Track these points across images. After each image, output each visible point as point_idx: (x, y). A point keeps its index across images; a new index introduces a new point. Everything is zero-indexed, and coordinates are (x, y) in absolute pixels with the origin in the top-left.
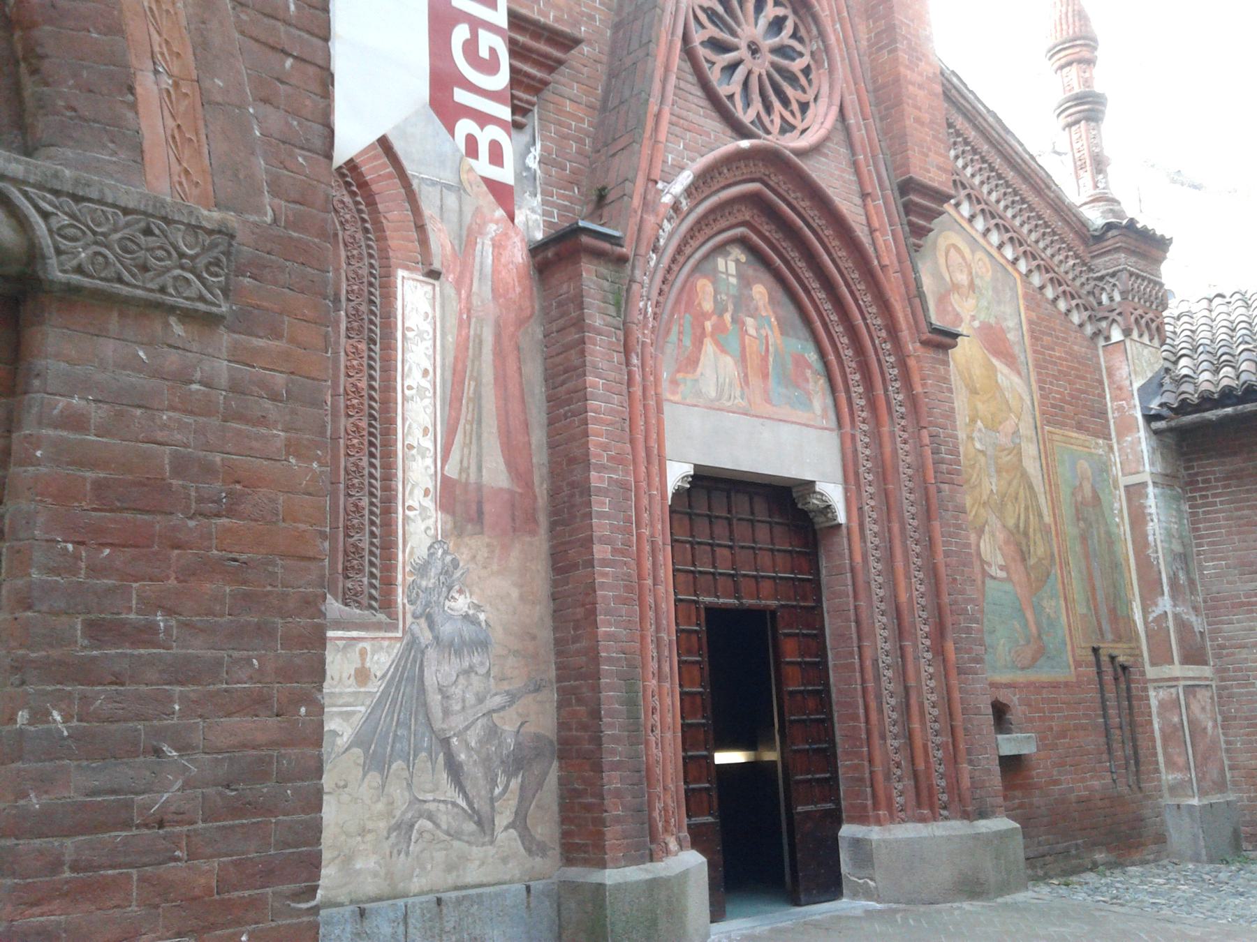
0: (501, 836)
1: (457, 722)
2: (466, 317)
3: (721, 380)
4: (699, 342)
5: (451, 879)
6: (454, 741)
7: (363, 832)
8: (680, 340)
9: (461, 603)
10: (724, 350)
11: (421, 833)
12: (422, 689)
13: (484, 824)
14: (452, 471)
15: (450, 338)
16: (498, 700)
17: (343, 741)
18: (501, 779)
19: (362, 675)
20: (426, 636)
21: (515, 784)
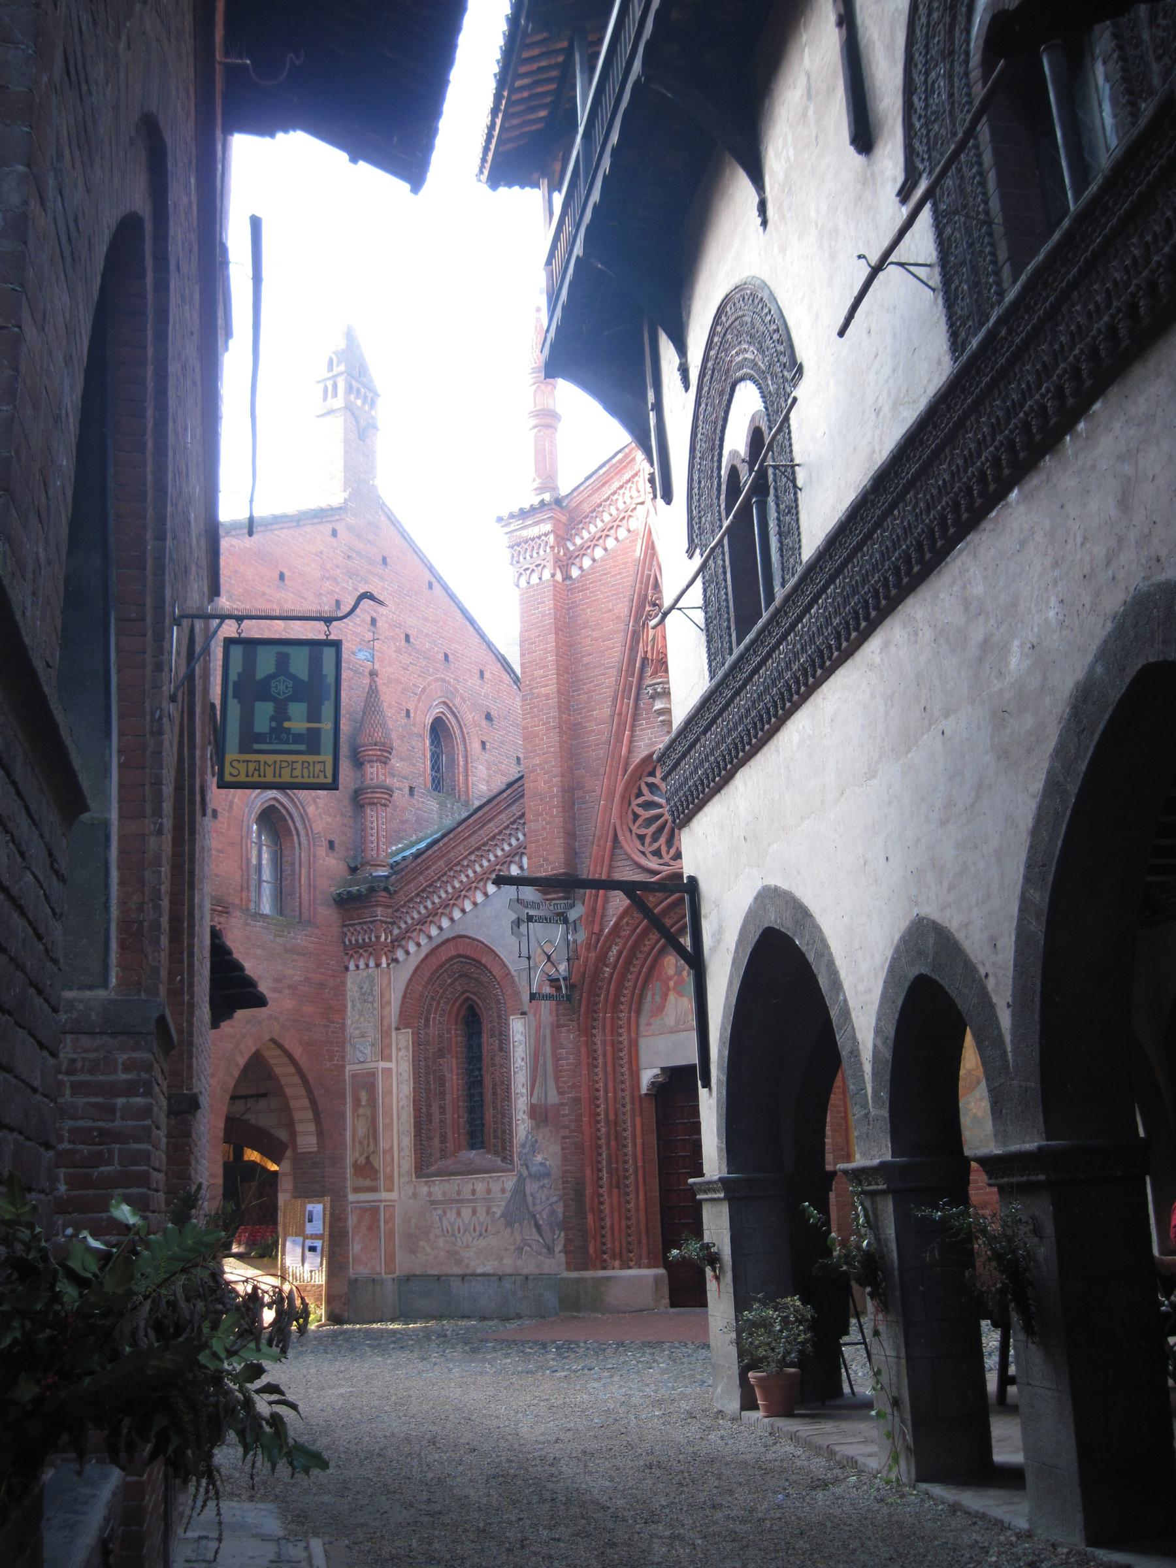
0: (557, 1255)
1: (539, 1208)
2: (538, 1028)
3: (679, 1013)
4: (665, 996)
5: (538, 1272)
6: (538, 1216)
7: (506, 1250)
8: (653, 998)
9: (539, 1158)
10: (680, 994)
11: (526, 1252)
12: (525, 1195)
13: (550, 1250)
14: (534, 1101)
15: (532, 1040)
16: (555, 1199)
17: (498, 1215)
18: (557, 1232)
19: (503, 1191)
20: (525, 1173)
21: (563, 1234)
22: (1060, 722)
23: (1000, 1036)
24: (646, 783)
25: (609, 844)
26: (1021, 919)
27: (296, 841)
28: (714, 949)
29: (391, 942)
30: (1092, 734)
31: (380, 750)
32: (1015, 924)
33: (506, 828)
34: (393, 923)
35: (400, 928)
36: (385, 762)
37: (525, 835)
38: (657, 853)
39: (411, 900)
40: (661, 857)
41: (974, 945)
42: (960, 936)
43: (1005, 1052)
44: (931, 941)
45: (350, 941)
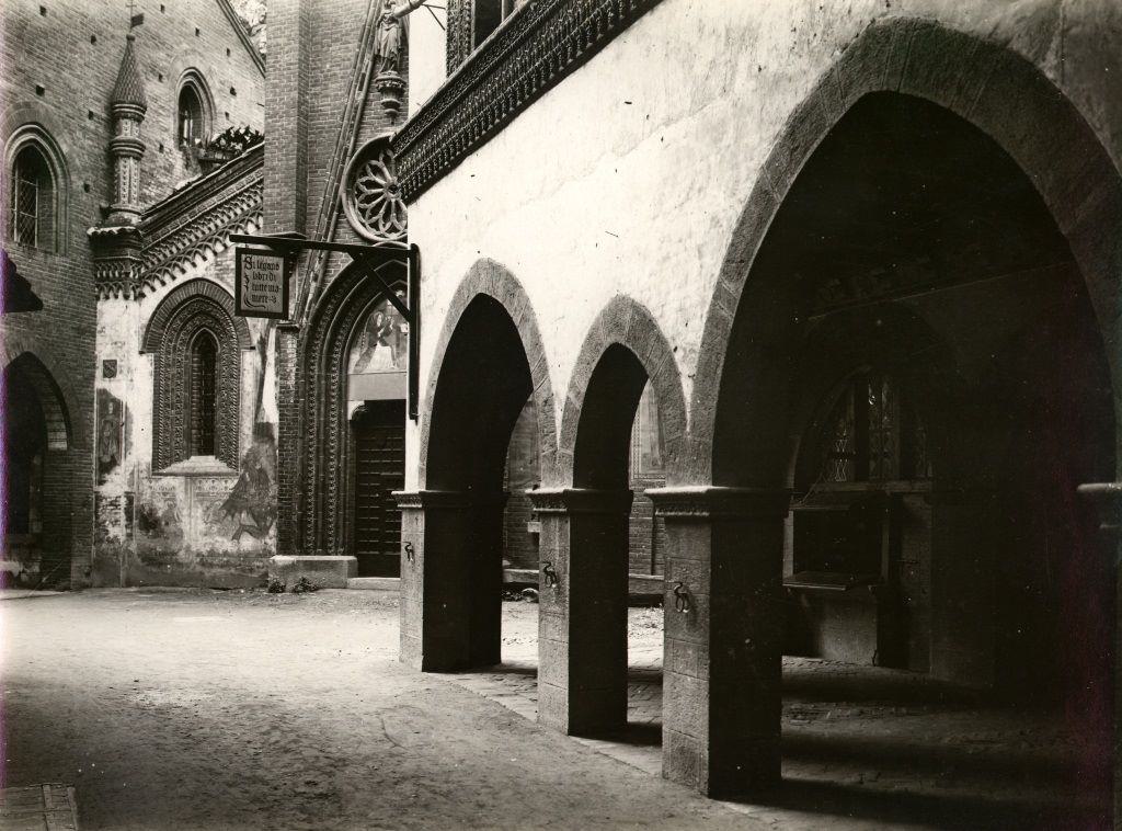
10: (385, 344)
22: (775, 138)
23: (682, 398)
24: (371, 166)
25: (335, 213)
26: (713, 305)
27: (54, 182)
28: (430, 307)
29: (140, 278)
30: (805, 152)
31: (135, 109)
32: (707, 308)
33: (246, 191)
34: (139, 263)
35: (147, 267)
36: (139, 120)
37: (262, 198)
38: (375, 226)
39: (158, 245)
40: (378, 229)
41: (668, 325)
42: (655, 314)
43: (684, 413)
44: (627, 317)
45: (101, 274)
